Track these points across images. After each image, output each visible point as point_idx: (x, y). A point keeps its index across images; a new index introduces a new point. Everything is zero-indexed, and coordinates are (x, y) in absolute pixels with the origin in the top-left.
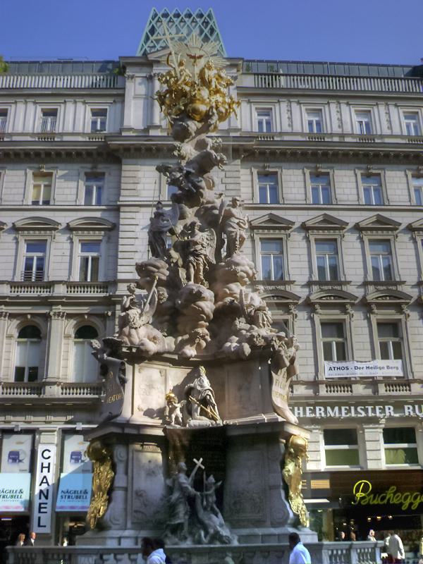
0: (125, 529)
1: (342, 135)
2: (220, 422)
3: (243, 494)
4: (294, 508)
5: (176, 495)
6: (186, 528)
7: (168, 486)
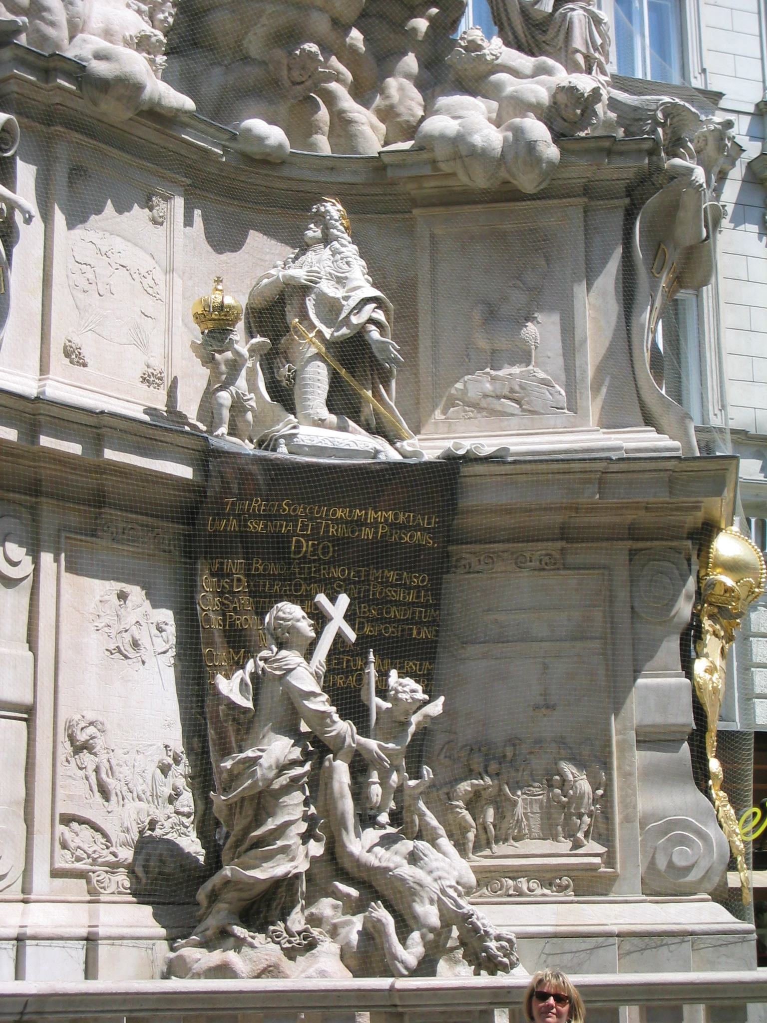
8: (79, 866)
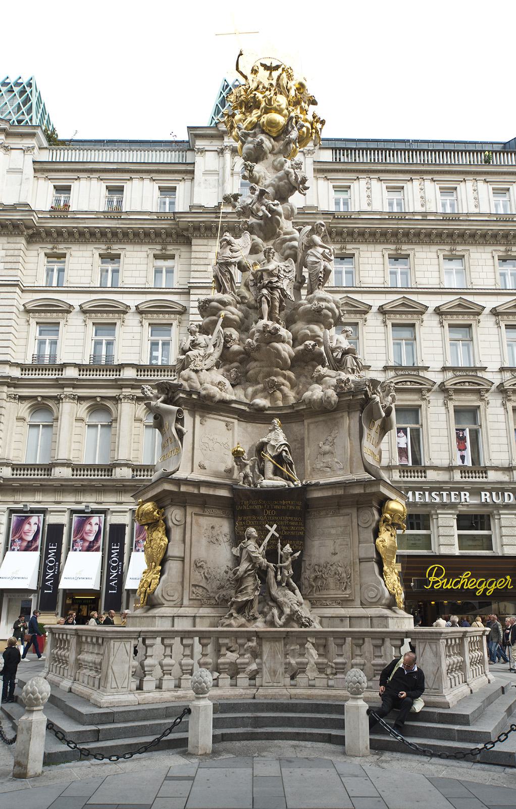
0: (181, 607)
2: (298, 483)
4: (390, 586)
5: (244, 566)
6: (256, 605)
7: (234, 556)
8: (198, 598)
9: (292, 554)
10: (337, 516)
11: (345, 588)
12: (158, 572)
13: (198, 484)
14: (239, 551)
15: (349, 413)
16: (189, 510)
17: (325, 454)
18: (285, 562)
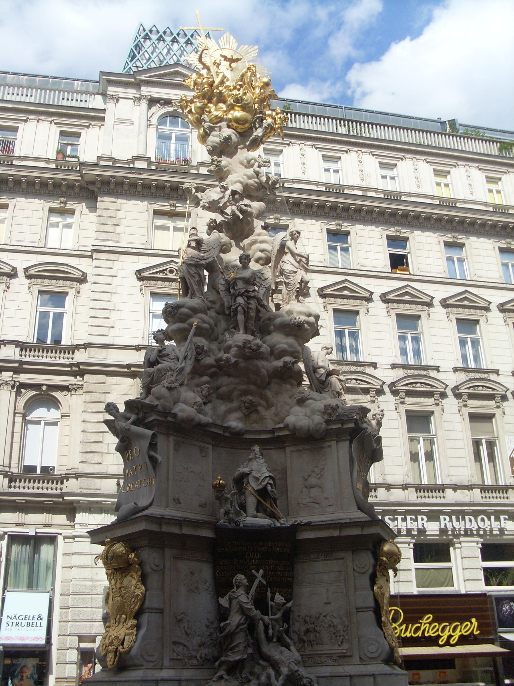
0: (162, 669)
1: (365, 189)
3: (318, 618)
5: (235, 619)
8: (179, 657)
9: (284, 604)
10: (330, 560)
11: (342, 642)
12: (132, 627)
13: (180, 522)
14: (228, 602)
15: (337, 442)
16: (168, 552)
17: (311, 487)
18: (276, 614)
